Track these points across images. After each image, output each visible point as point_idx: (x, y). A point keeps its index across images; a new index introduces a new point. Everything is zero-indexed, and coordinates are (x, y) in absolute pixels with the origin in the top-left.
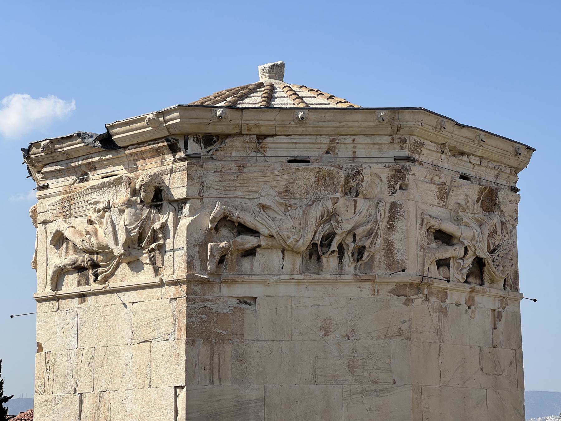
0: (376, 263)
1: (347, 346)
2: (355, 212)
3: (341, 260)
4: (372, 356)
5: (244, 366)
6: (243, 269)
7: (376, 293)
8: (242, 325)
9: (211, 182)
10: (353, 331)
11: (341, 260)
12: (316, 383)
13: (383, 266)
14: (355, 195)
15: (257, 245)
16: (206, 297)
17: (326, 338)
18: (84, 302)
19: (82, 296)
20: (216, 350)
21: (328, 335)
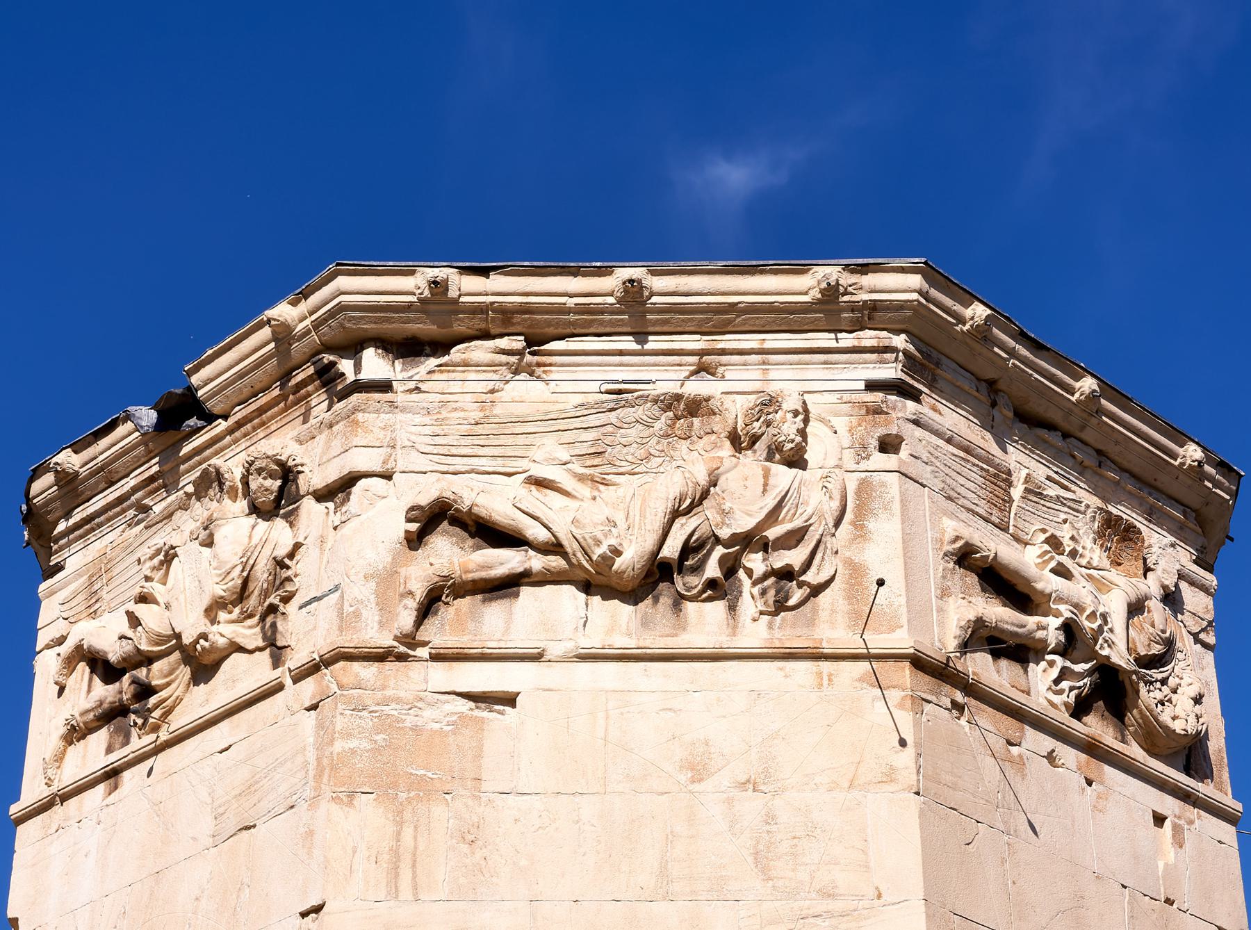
0: (824, 615)
1: (751, 805)
2: (765, 491)
3: (732, 608)
4: (819, 831)
5: (479, 854)
6: (485, 629)
7: (825, 682)
8: (478, 756)
9: (413, 438)
10: (766, 771)
11: (732, 608)
12: (668, 898)
13: (841, 619)
14: (764, 455)
15: (521, 570)
16: (389, 693)
17: (696, 787)
18: (116, 788)
19: (112, 775)
20: (408, 815)
21: (701, 780)
